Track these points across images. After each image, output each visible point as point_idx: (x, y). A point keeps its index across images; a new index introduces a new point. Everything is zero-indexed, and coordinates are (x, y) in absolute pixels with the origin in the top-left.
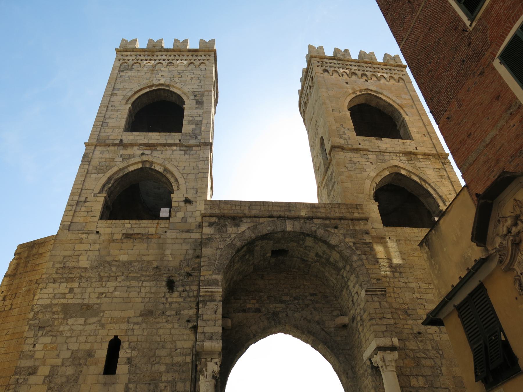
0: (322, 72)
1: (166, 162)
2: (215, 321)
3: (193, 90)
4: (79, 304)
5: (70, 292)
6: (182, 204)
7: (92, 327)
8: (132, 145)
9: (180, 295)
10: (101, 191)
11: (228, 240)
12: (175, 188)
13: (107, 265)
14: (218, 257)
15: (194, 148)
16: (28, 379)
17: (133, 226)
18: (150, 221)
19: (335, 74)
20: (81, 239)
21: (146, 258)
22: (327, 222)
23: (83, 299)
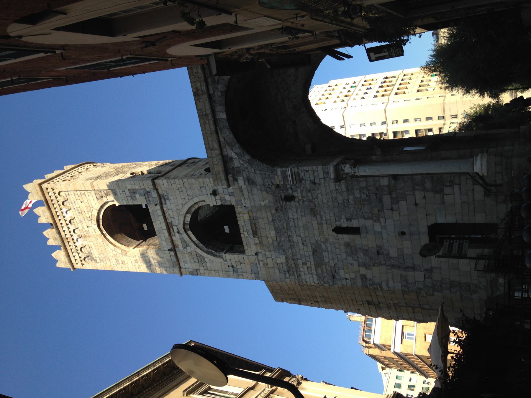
1: (181, 213)
2: (314, 171)
3: (96, 200)
4: (314, 258)
5: (306, 265)
6: (218, 197)
7: (329, 247)
8: (172, 242)
9: (295, 191)
10: (221, 257)
11: (246, 165)
12: (204, 203)
13: (281, 244)
14: (262, 172)
15: (160, 192)
16: (370, 279)
17: (245, 230)
18: (238, 219)
20: (264, 264)
21: (270, 218)
22: (209, 80)
23: (309, 255)
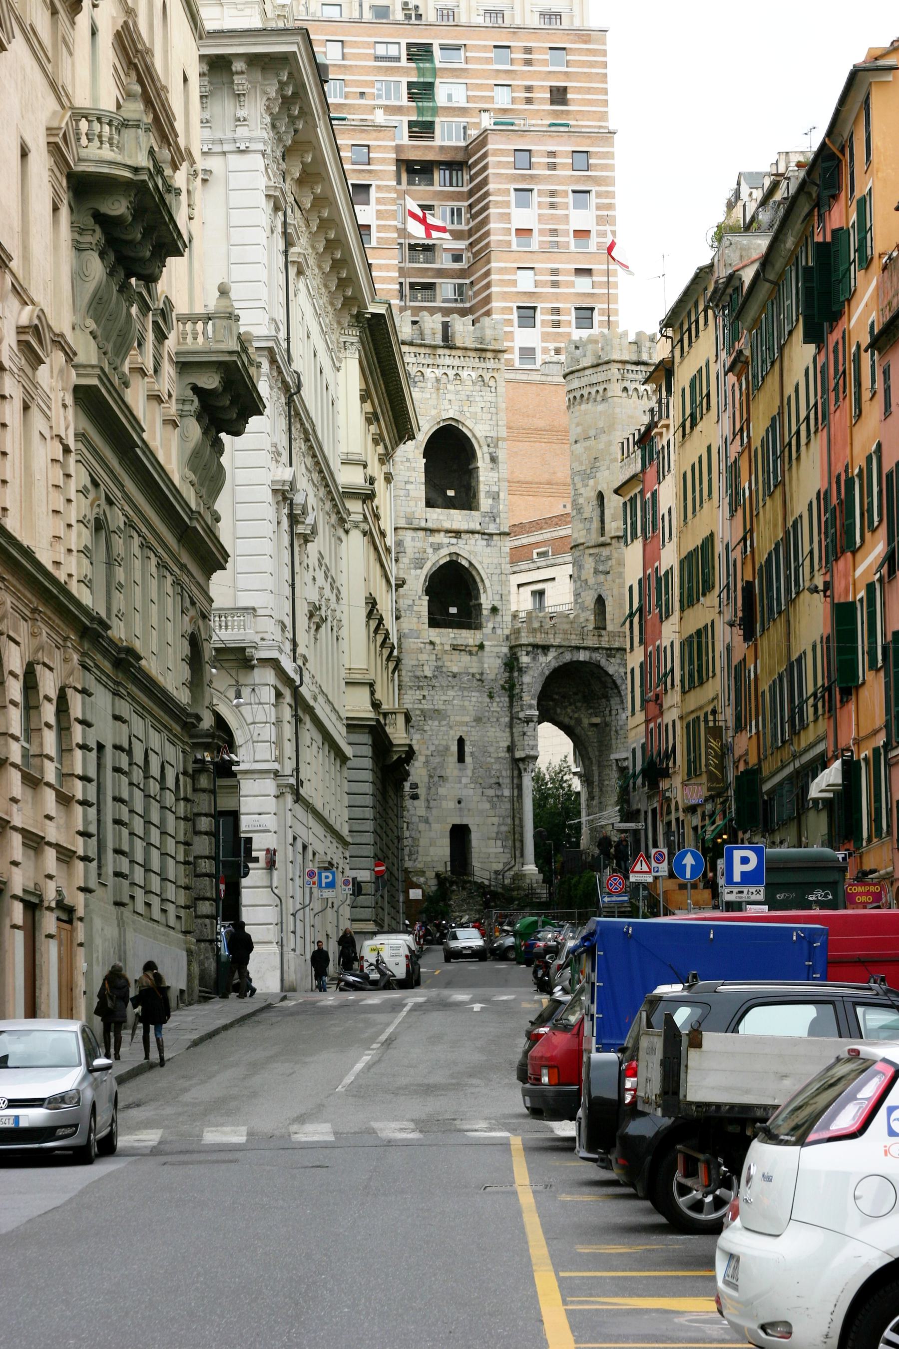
0: (620, 393)
3: (485, 434)
8: (438, 531)
12: (482, 591)
19: (635, 394)
21: (471, 671)
